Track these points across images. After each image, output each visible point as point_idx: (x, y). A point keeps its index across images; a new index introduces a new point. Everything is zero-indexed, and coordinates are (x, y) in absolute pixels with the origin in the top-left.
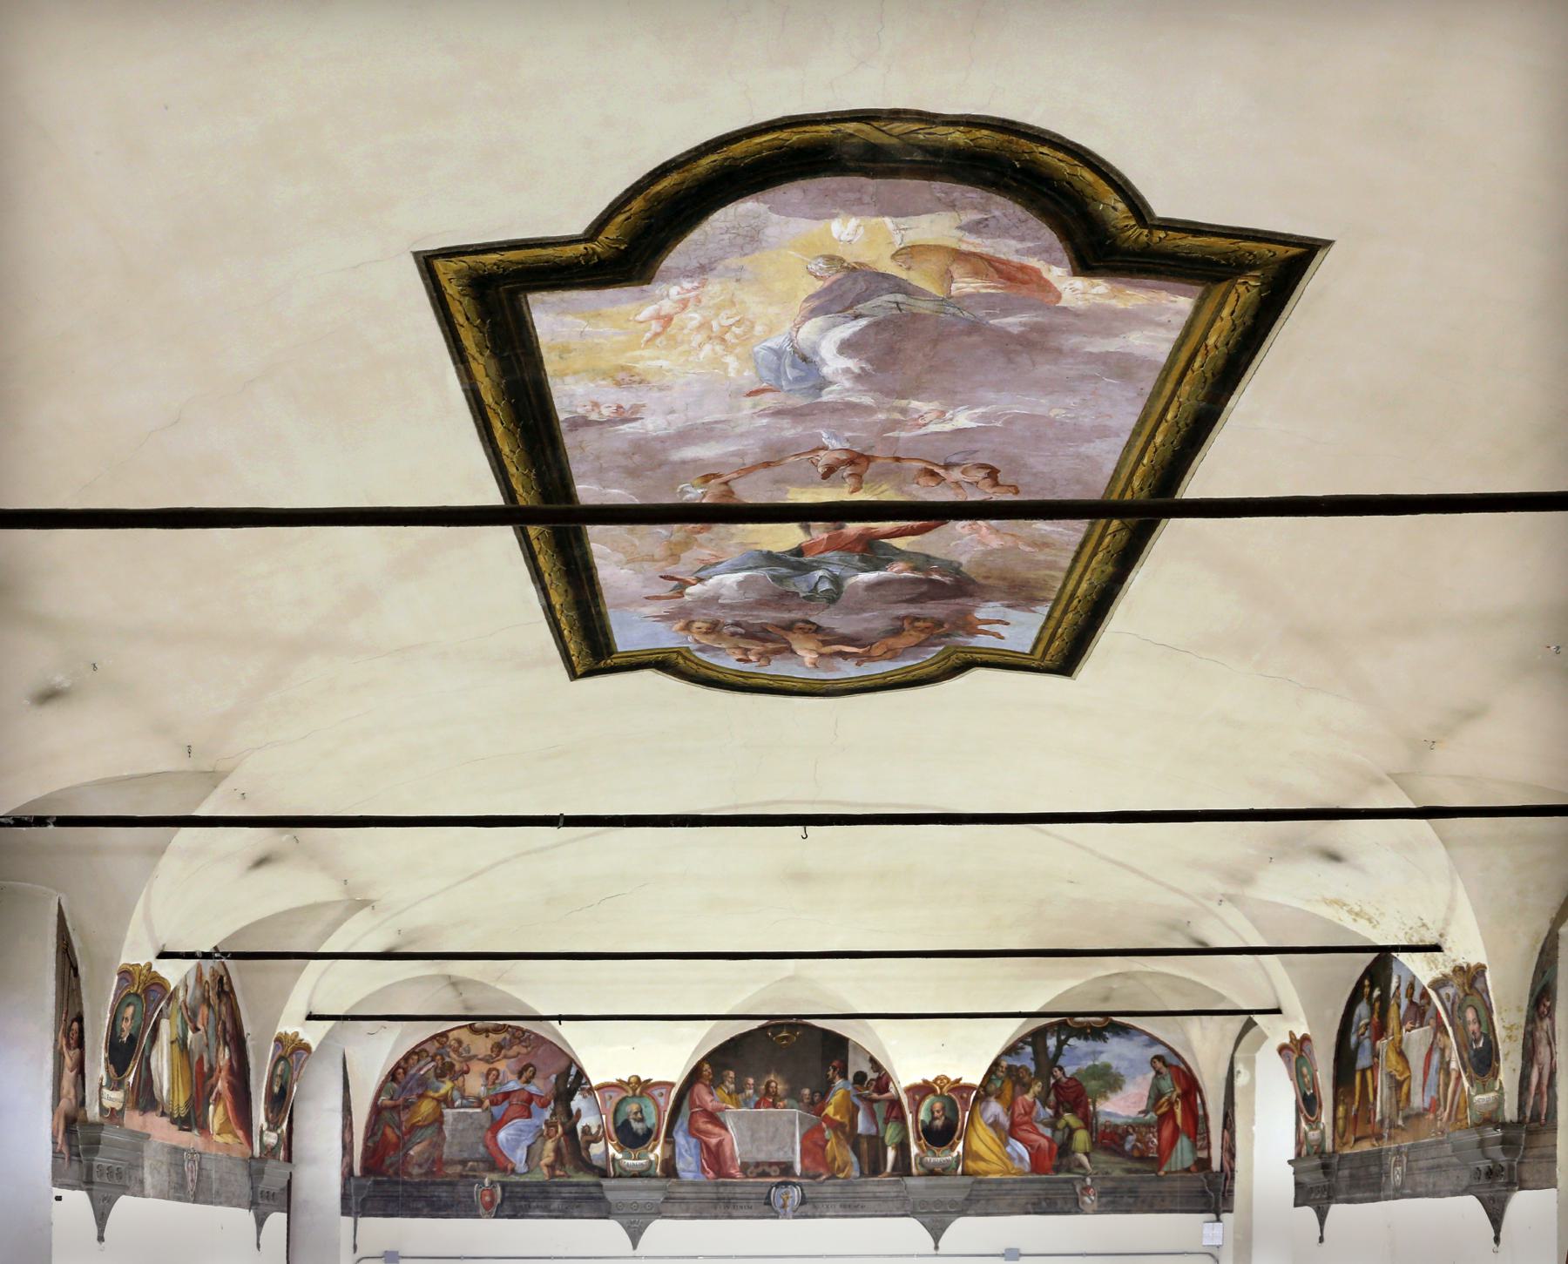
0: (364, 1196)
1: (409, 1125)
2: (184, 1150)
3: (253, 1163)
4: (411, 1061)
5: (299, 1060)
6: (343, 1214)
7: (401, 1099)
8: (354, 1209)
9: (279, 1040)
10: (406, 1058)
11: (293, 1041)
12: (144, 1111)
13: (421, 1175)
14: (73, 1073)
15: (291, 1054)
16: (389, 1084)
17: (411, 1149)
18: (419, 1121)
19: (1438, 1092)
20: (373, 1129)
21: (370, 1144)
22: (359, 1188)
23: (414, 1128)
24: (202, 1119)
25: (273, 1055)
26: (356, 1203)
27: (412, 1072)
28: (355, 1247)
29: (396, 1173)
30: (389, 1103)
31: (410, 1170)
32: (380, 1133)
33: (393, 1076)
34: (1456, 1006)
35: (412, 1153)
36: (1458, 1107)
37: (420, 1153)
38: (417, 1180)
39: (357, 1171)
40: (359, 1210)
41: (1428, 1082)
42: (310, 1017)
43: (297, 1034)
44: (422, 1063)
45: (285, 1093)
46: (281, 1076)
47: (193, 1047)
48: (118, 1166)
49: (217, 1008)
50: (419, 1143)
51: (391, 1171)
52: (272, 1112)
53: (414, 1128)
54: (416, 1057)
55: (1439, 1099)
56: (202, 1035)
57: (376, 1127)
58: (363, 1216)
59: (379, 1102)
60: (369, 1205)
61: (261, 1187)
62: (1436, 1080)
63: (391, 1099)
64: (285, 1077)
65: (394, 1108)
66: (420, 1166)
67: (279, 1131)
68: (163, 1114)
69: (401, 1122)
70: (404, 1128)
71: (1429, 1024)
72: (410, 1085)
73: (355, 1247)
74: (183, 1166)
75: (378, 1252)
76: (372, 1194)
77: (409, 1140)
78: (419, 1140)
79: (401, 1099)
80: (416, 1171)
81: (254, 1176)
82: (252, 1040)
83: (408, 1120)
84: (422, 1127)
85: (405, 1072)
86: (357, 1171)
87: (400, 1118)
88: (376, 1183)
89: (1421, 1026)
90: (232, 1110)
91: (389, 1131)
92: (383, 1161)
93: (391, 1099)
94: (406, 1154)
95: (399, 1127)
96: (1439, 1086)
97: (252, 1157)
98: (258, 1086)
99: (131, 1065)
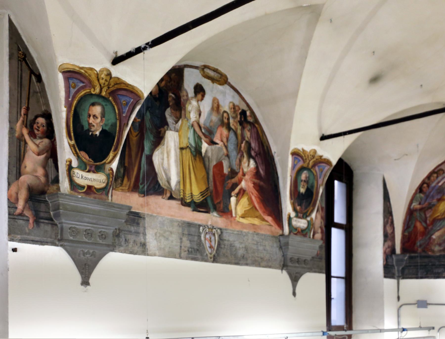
0: (403, 266)
1: (431, 219)
2: (200, 226)
3: (281, 239)
4: (432, 178)
5: (322, 172)
6: (385, 277)
7: (426, 203)
8: (397, 274)
9: (295, 154)
10: (429, 177)
11: (313, 157)
12: (146, 193)
13: (440, 251)
14: (42, 157)
15: (314, 166)
16: (418, 195)
17: (433, 234)
18: (438, 216)
20: (408, 222)
21: (406, 234)
22: (399, 261)
23: (435, 221)
24: (222, 205)
25: (294, 166)
26: (398, 271)
27: (433, 185)
28: (399, 298)
29: (424, 251)
30: (418, 207)
31: (433, 248)
32: (412, 226)
33: (420, 189)
35: (434, 237)
37: (439, 237)
38: (438, 254)
39: (398, 250)
40: (400, 275)
42: (323, 138)
43: (315, 152)
44: (440, 178)
45: (312, 193)
46: (307, 181)
47: (210, 154)
48: (100, 230)
49: (239, 132)
50: (439, 230)
51: (420, 250)
52: (300, 205)
53: (435, 221)
54: (435, 175)
56: (220, 149)
57: (410, 223)
58: (404, 278)
59: (412, 207)
60: (406, 271)
61: (290, 254)
63: (420, 204)
64: (311, 182)
65: (421, 209)
66: (440, 245)
67: (309, 219)
68: (171, 198)
69: (426, 218)
70: (428, 222)
72: (432, 193)
73: (399, 298)
74: (199, 236)
75: (413, 301)
76: (408, 265)
77: (432, 229)
78: (438, 228)
79: (426, 203)
80: (437, 248)
81: (283, 248)
82: (278, 156)
83: (430, 216)
84: (440, 220)
85: (428, 186)
86: (398, 250)
87: (425, 215)
88: (411, 258)
90: (258, 203)
91: (418, 224)
92: (415, 244)
93: (420, 204)
94: (430, 238)
95: (426, 222)
97: (282, 235)
98: (285, 188)
99: (111, 155)
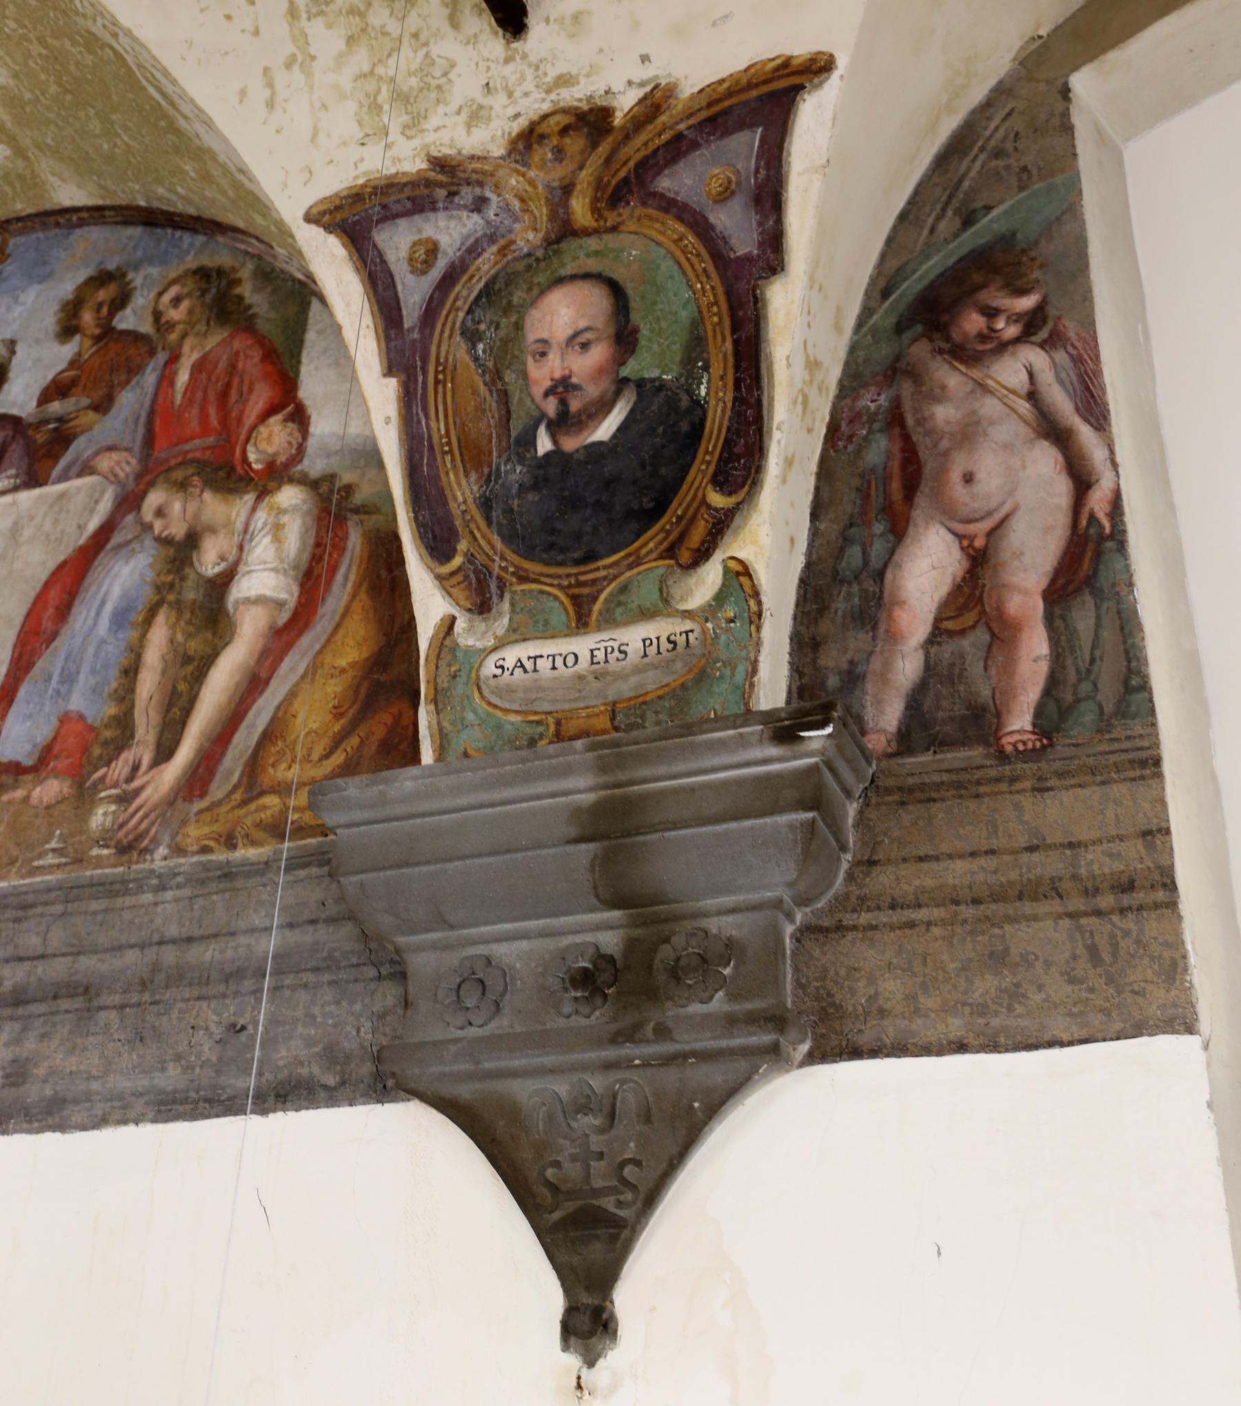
19: (126, 694)
34: (466, 291)
36: (268, 736)
41: (51, 662)
55: (124, 726)
62: (115, 652)
71: (87, 469)
89: (33, 479)
96: (131, 672)
